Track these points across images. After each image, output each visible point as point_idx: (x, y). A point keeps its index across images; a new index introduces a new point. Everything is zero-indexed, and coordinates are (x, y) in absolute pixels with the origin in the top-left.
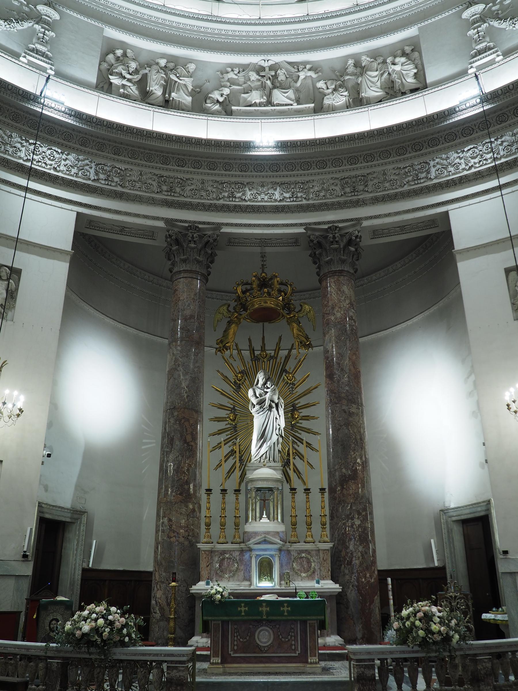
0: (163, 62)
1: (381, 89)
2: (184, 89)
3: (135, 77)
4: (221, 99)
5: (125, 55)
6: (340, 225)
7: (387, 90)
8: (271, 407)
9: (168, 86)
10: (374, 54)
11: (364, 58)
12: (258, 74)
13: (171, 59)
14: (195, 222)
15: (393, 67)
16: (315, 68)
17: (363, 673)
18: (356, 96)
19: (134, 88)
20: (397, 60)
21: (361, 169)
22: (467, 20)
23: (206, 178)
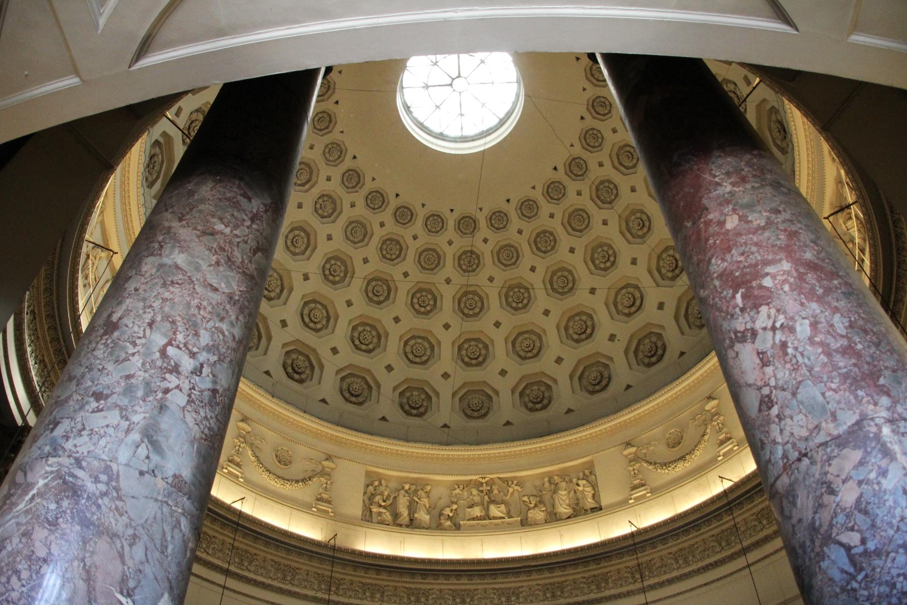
0: (407, 487)
1: (569, 505)
4: (451, 515)
5: (381, 484)
10: (564, 475)
11: (556, 478)
13: (414, 482)
16: (520, 483)
19: (388, 514)
20: (580, 482)
21: (557, 577)
22: (626, 456)
23: (443, 587)
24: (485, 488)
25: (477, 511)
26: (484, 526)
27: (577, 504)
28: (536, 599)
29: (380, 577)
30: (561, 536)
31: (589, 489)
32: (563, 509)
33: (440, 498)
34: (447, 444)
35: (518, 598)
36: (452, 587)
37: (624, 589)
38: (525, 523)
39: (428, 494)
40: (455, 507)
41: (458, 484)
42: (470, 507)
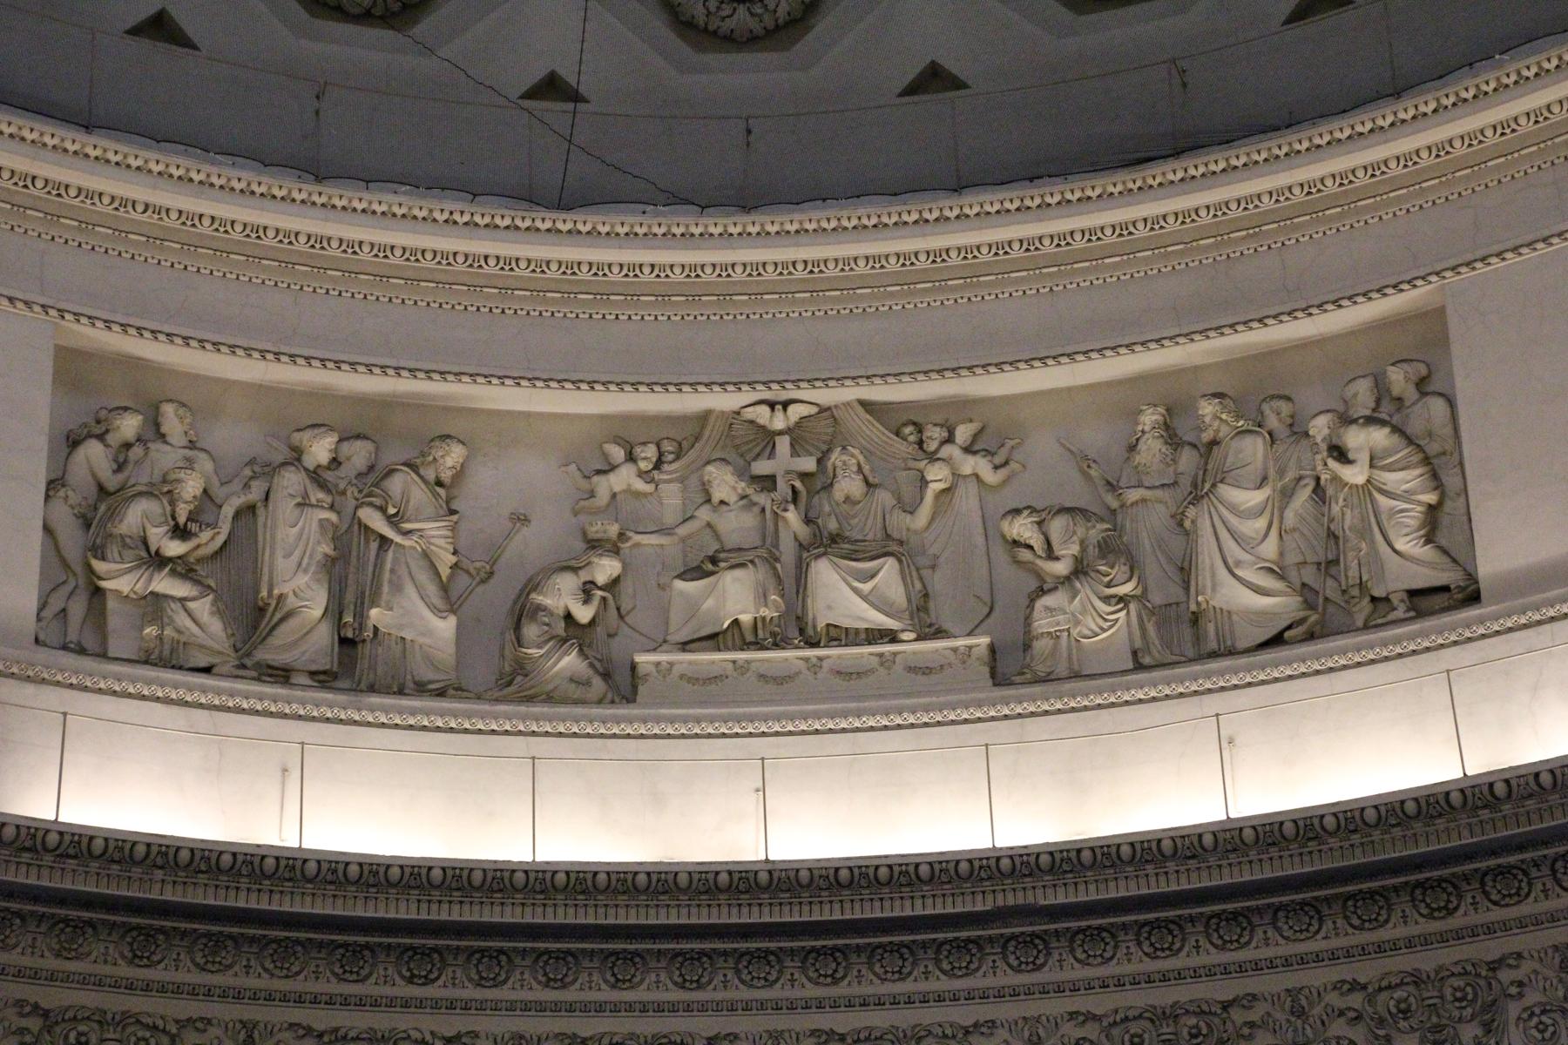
0: (320, 450)
1: (1278, 571)
2: (423, 577)
3: (205, 536)
4: (583, 614)
5: (155, 431)
7: (1309, 576)
9: (352, 570)
10: (1258, 394)
12: (743, 473)
13: (358, 421)
15: (1332, 463)
16: (994, 435)
18: (1176, 592)
19: (203, 607)
20: (1358, 439)
24: (783, 461)
25: (736, 596)
26: (779, 680)
27: (1329, 566)
29: (156, 974)
30: (1225, 743)
31: (1406, 479)
32: (1244, 594)
33: (521, 519)
34: (564, 202)
39: (446, 490)
40: (605, 569)
41: (627, 436)
42: (695, 572)
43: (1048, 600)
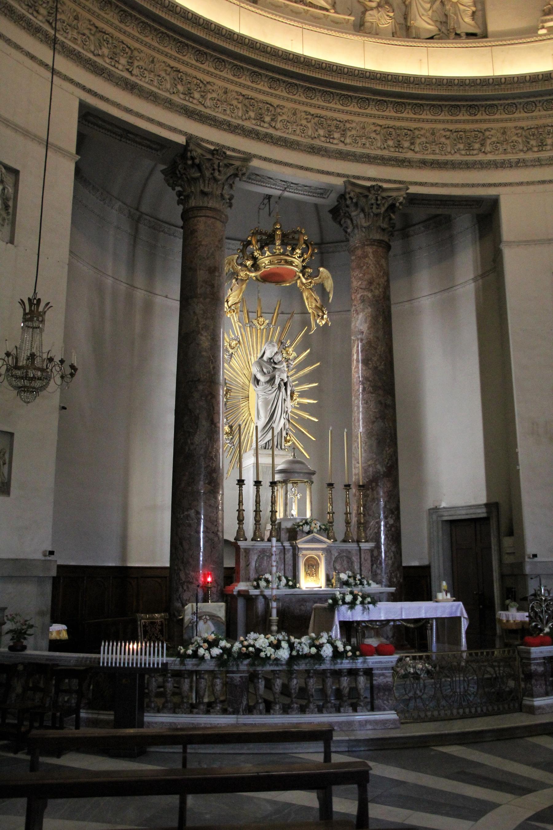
6: (385, 185)
8: (279, 388)
14: (224, 146)
17: (536, 669)
18: (402, 21)
21: (406, 119)
28: (372, 144)
35: (343, 135)
36: (245, 92)
37: (513, 157)
38: (360, 27)
43: (370, 12)
